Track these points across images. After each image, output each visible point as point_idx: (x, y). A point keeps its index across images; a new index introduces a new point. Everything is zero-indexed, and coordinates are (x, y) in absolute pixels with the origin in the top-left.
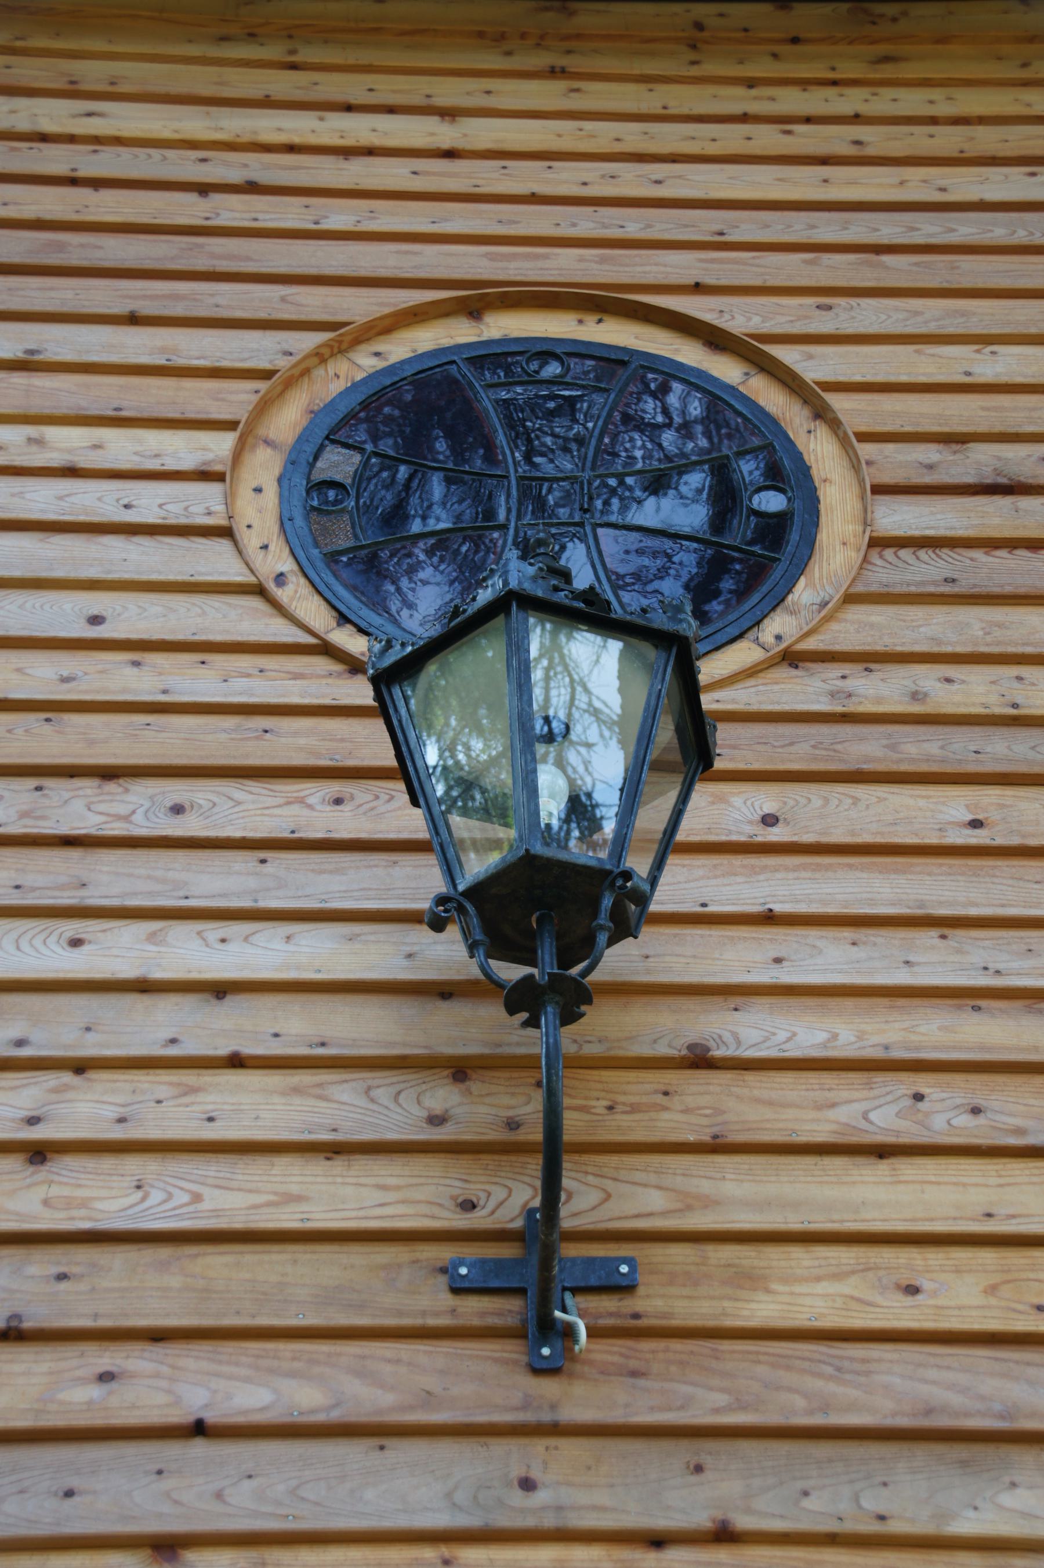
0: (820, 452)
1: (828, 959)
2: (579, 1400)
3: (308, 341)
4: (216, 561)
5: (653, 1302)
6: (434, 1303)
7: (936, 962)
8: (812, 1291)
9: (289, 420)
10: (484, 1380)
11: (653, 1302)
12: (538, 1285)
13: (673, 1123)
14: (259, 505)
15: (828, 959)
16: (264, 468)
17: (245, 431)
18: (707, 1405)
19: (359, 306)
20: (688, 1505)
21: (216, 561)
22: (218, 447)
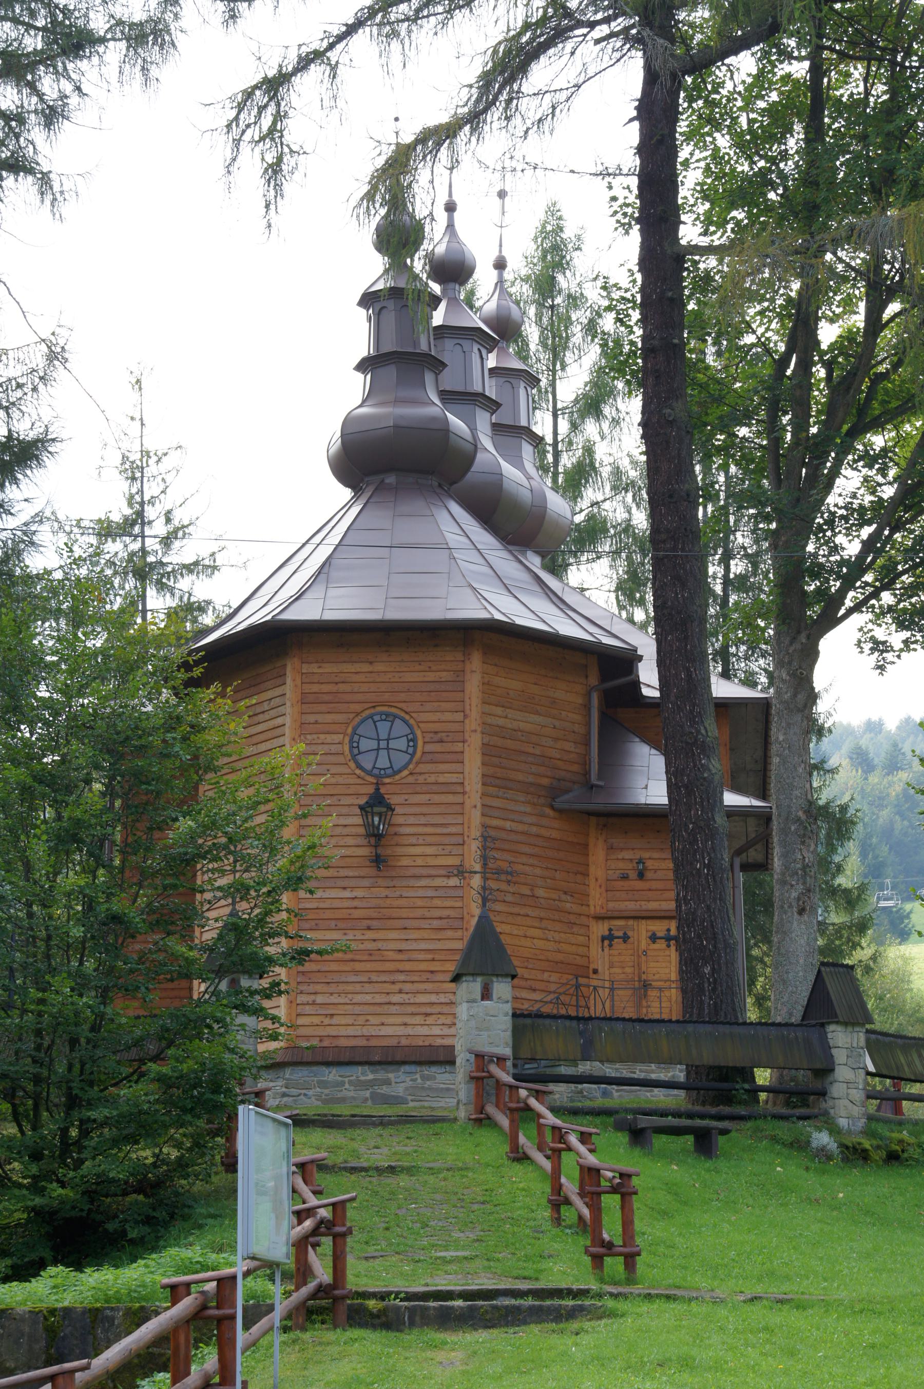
0: (419, 733)
1: (412, 820)
2: (381, 874)
3: (351, 716)
4: (341, 759)
5: (390, 863)
6: (368, 863)
7: (423, 820)
8: (405, 862)
9: (350, 730)
10: (372, 871)
11: (390, 863)
12: (378, 861)
13: (392, 843)
14: (347, 748)
15: (412, 820)
16: (347, 740)
17: (345, 734)
18: (394, 874)
19: (358, 707)
20: (391, 884)
21: (341, 759)
22: (341, 736)
